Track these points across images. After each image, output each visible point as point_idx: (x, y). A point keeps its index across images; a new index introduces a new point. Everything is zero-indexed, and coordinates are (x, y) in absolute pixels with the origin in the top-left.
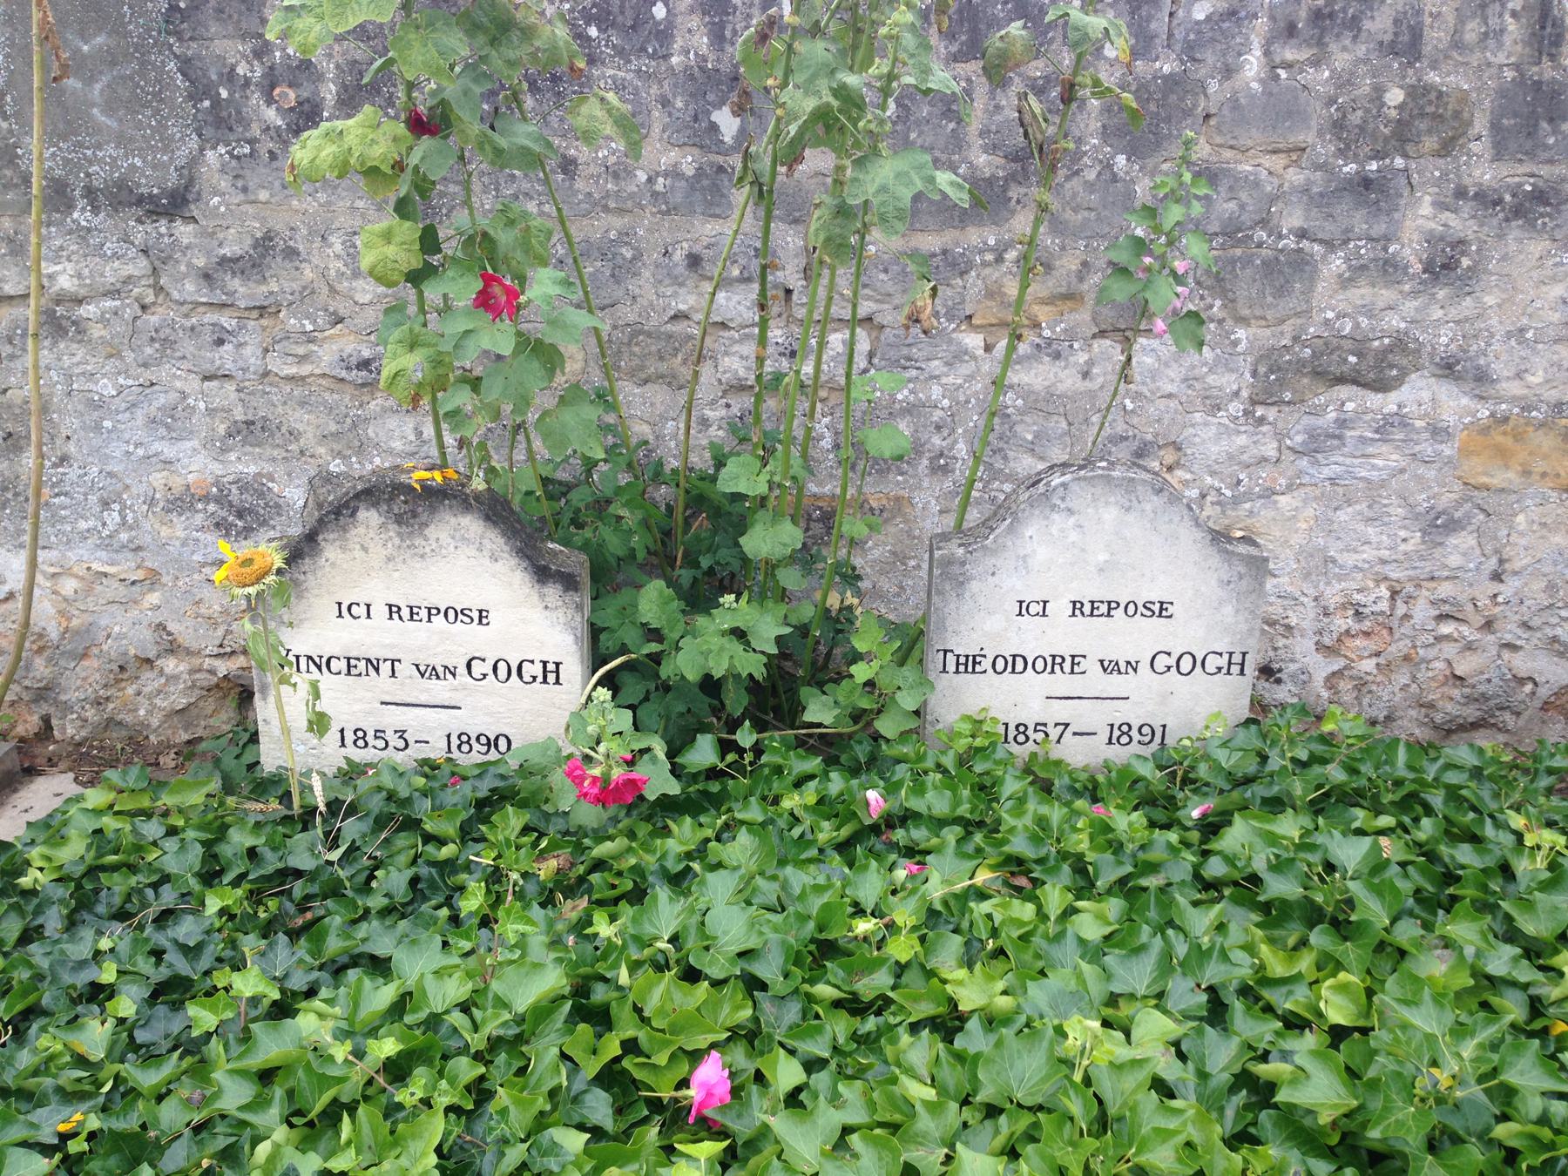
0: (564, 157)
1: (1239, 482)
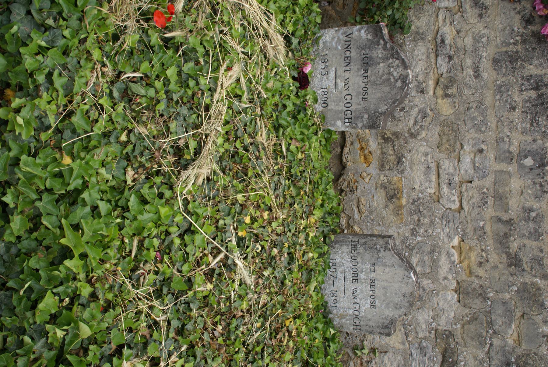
0: (515, 108)
1: (410, 326)
